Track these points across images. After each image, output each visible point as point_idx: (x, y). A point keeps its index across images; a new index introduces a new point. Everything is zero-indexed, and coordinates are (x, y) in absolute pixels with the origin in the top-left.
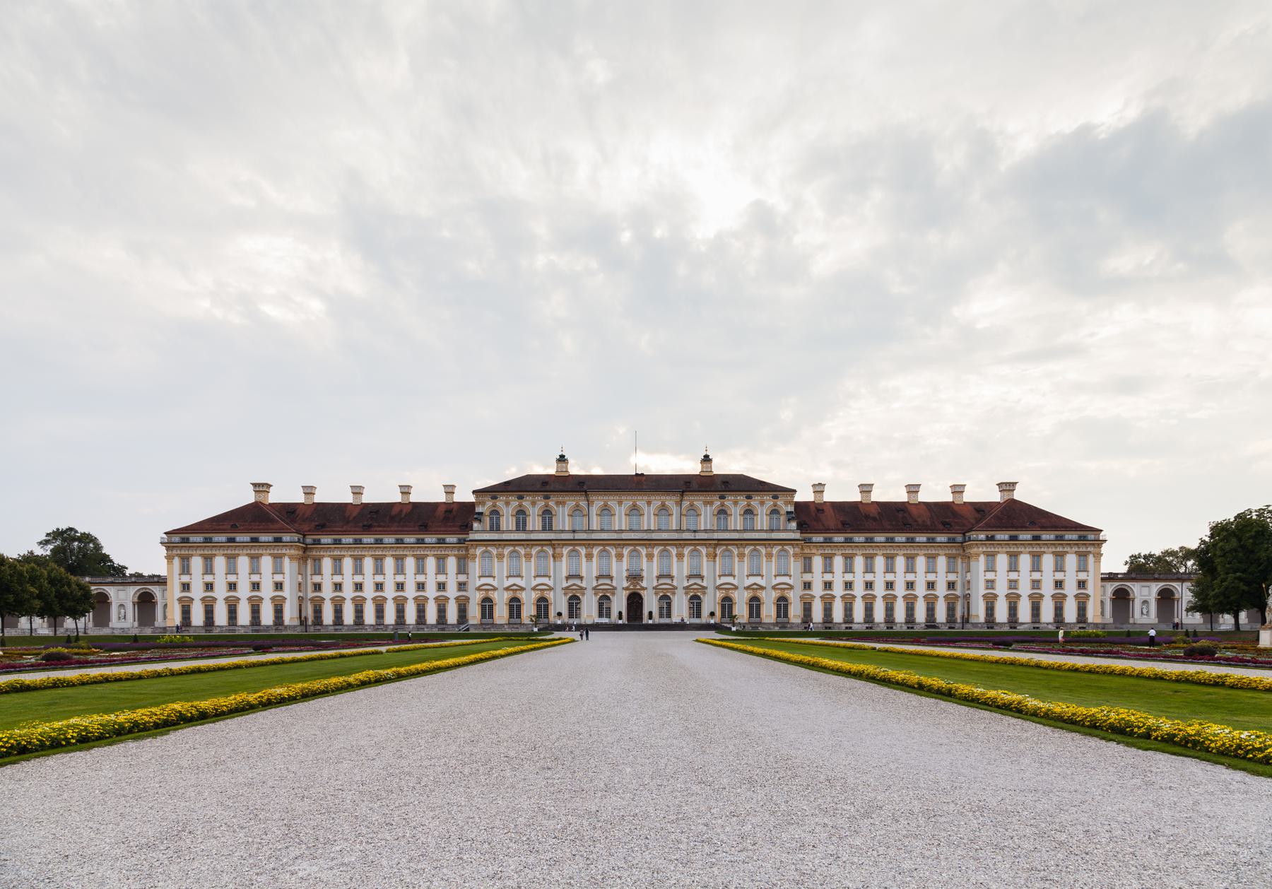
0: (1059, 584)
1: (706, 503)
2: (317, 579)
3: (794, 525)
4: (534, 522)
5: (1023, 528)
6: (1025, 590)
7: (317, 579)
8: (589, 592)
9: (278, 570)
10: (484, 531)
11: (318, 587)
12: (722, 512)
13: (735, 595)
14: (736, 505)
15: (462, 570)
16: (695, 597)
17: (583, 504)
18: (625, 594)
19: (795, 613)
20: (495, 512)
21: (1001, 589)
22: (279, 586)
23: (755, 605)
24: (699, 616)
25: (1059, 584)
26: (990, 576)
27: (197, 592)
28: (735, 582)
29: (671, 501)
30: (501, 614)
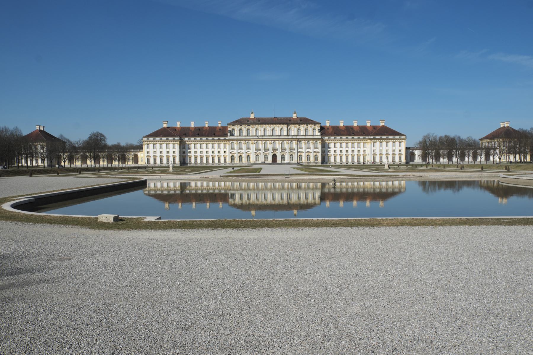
0: (394, 151)
1: (295, 127)
3: (319, 134)
4: (244, 133)
5: (384, 135)
6: (384, 152)
7: (184, 150)
8: (262, 153)
10: (230, 136)
12: (299, 129)
14: (303, 127)
16: (291, 155)
20: (233, 129)
21: (378, 152)
22: (174, 152)
23: (308, 157)
25: (394, 151)
26: (375, 148)
27: (151, 154)
28: (303, 150)
29: (285, 127)
30: (236, 160)
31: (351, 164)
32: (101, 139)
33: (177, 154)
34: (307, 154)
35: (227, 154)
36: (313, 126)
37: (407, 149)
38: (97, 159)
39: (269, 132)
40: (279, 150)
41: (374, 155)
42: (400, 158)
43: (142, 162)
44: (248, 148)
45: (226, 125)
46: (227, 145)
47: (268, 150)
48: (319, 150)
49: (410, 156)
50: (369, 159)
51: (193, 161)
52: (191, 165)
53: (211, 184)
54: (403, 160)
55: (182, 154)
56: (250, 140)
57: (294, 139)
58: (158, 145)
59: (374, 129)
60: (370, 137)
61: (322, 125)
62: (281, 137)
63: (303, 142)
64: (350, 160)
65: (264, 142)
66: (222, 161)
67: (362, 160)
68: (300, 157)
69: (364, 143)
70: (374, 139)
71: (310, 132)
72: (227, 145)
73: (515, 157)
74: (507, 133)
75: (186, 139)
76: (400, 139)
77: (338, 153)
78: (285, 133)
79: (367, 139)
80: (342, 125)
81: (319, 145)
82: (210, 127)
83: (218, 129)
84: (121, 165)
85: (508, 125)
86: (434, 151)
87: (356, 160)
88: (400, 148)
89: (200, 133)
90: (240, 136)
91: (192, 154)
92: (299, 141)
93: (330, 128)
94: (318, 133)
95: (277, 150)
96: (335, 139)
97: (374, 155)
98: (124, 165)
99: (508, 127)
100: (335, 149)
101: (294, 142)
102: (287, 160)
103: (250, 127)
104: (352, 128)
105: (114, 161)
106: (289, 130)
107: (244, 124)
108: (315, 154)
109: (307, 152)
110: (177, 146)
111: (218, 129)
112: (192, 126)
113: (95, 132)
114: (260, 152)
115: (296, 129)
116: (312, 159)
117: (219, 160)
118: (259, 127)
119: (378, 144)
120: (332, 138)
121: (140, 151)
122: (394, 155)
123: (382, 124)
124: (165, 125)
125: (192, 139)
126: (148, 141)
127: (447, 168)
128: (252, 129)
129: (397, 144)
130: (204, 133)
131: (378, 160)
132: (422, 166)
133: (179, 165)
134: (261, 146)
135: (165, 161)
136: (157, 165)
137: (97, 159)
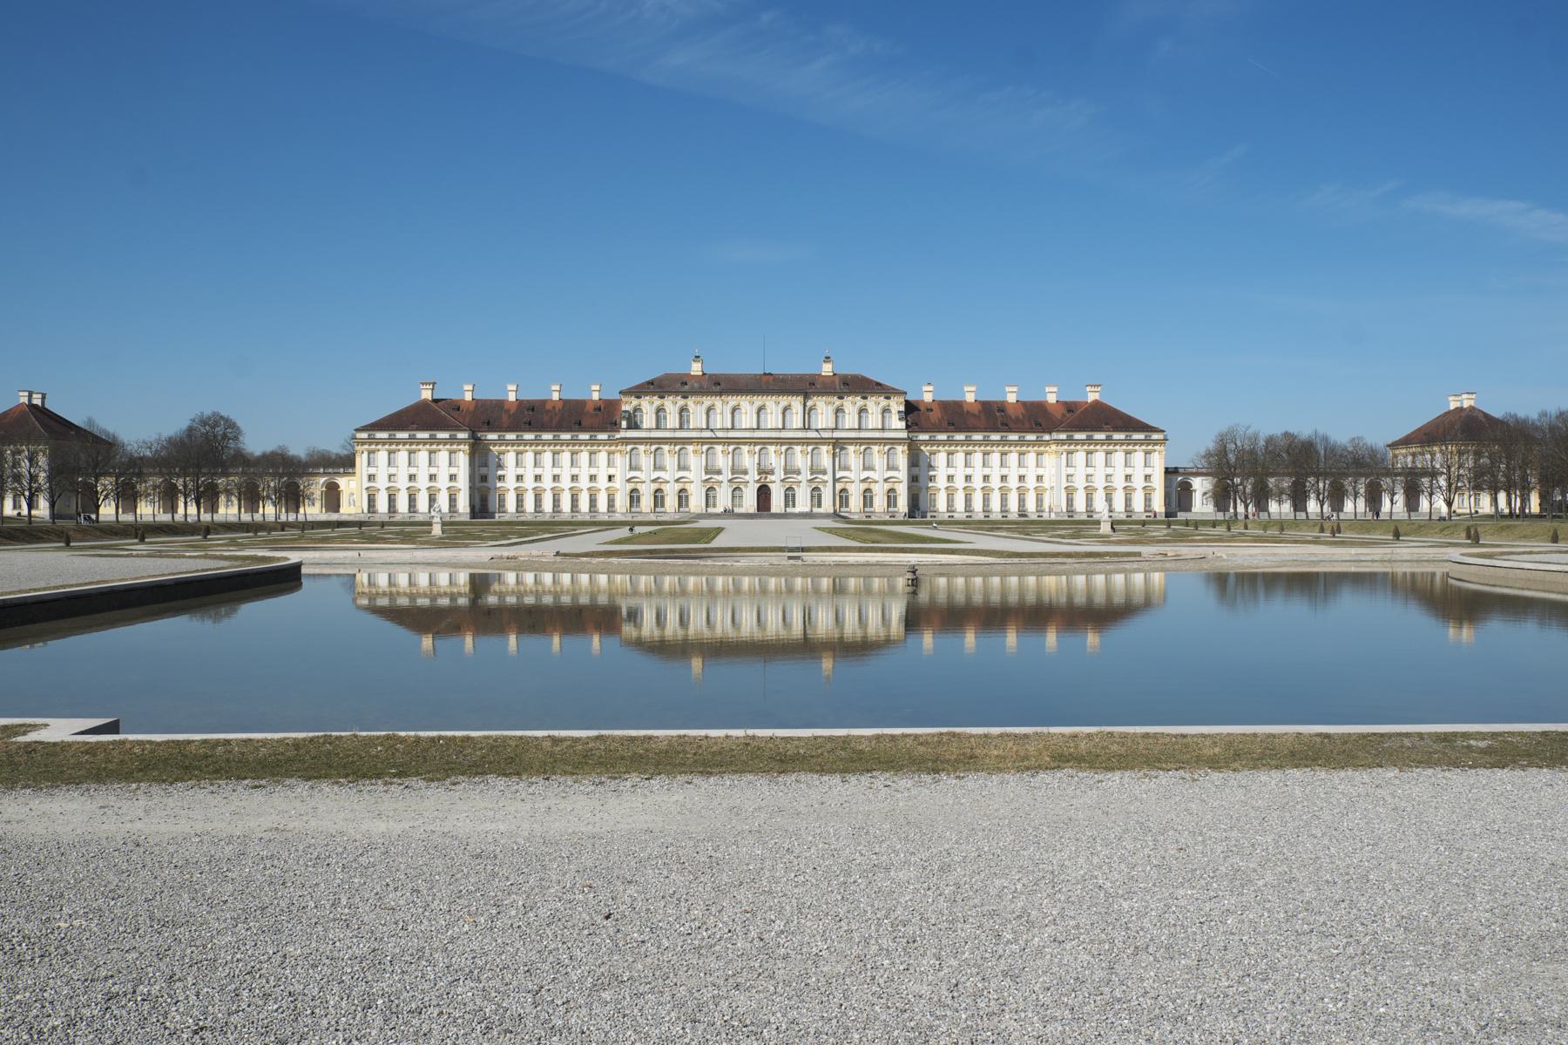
0: (1128, 477)
2: (483, 471)
3: (903, 425)
4: (672, 420)
5: (1100, 429)
6: (1099, 483)
7: (483, 471)
8: (725, 484)
10: (629, 428)
12: (839, 411)
14: (851, 404)
21: (1079, 483)
22: (452, 477)
24: (819, 505)
25: (1128, 477)
26: (1070, 471)
27: (382, 483)
29: (796, 403)
30: (646, 503)
31: (999, 517)
32: (225, 436)
33: (463, 483)
34: (864, 486)
35: (618, 483)
36: (883, 402)
37: (1170, 472)
38: (208, 496)
39: (747, 419)
40: (779, 474)
41: (1070, 492)
42: (1148, 500)
43: (352, 505)
44: (682, 467)
45: (617, 396)
46: (618, 455)
47: (745, 472)
48: (902, 474)
49: (1179, 496)
50: (1055, 504)
51: (511, 505)
52: (506, 518)
53: (529, 578)
54: (1158, 505)
55: (478, 484)
56: (689, 441)
57: (823, 441)
58: (402, 456)
59: (1069, 411)
60: (1055, 436)
62: (784, 434)
63: (851, 448)
64: (995, 505)
65: (731, 448)
66: (602, 505)
67: (1031, 506)
68: (843, 497)
69: (1039, 454)
70: (1070, 441)
71: (873, 420)
72: (618, 455)
73: (1495, 501)
74: (1468, 428)
75: (492, 436)
76: (1147, 442)
77: (960, 483)
78: (796, 420)
79: (1047, 443)
80: (970, 398)
81: (901, 457)
82: (565, 403)
83: (590, 408)
84: (283, 518)
85: (1472, 403)
86: (1252, 480)
87: (1013, 505)
88: (1148, 471)
89: (535, 418)
90: (658, 428)
91: (510, 483)
92: (838, 445)
93: (935, 407)
94: (896, 423)
95: (772, 472)
96: (950, 442)
97: (1070, 492)
98: (292, 517)
99: (1472, 408)
100: (951, 471)
101: (824, 448)
102: (803, 504)
103: (690, 402)
104: (1002, 407)
105: (222, 498)
106: (808, 412)
107: (670, 393)
108: (887, 486)
109: (864, 481)
110: (463, 459)
111: (590, 408)
112: (512, 397)
113: (208, 412)
114: (720, 478)
115: (831, 409)
116: (879, 503)
117: (593, 502)
118: (717, 402)
119: (1080, 457)
120: (942, 437)
121: (346, 474)
122: (1129, 491)
123: (1092, 397)
124: (427, 394)
125: (511, 436)
126: (371, 441)
127: (1289, 533)
128: (697, 409)
129: (1138, 457)
130: (546, 419)
131: (1080, 505)
132: (1214, 524)
133: (467, 518)
134: (722, 460)
135: (422, 504)
136: (398, 518)
137: (208, 496)
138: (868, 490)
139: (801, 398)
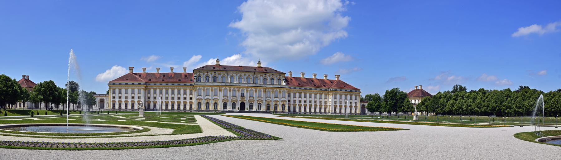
2: (149, 95)
4: (211, 79)
7: (149, 95)
9: (139, 93)
10: (197, 82)
11: (149, 98)
13: (271, 103)
15: (191, 94)
17: (226, 74)
18: (240, 102)
19: (286, 109)
22: (139, 98)
29: (251, 75)
35: (193, 100)
61: (286, 76)
110: (142, 91)
138: (276, 104)
139: (253, 74)
